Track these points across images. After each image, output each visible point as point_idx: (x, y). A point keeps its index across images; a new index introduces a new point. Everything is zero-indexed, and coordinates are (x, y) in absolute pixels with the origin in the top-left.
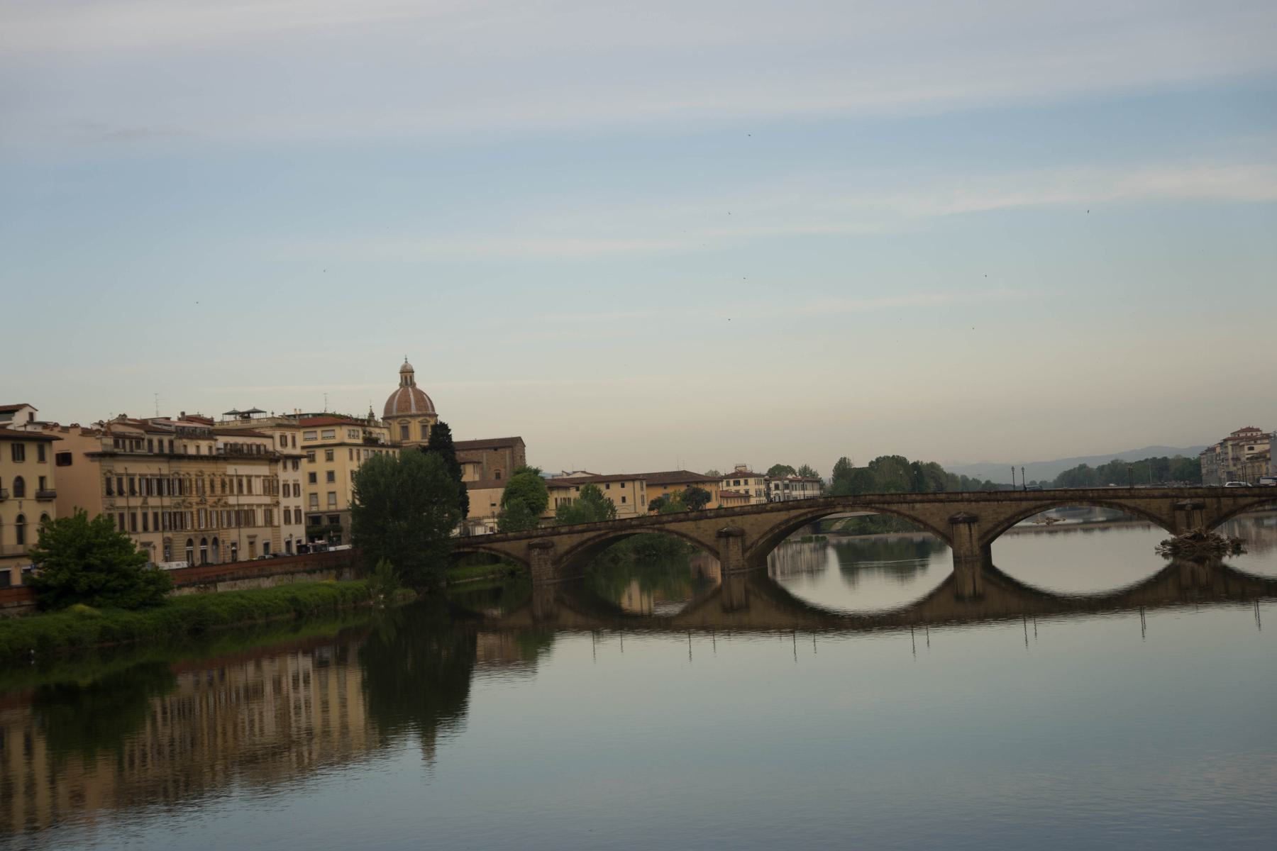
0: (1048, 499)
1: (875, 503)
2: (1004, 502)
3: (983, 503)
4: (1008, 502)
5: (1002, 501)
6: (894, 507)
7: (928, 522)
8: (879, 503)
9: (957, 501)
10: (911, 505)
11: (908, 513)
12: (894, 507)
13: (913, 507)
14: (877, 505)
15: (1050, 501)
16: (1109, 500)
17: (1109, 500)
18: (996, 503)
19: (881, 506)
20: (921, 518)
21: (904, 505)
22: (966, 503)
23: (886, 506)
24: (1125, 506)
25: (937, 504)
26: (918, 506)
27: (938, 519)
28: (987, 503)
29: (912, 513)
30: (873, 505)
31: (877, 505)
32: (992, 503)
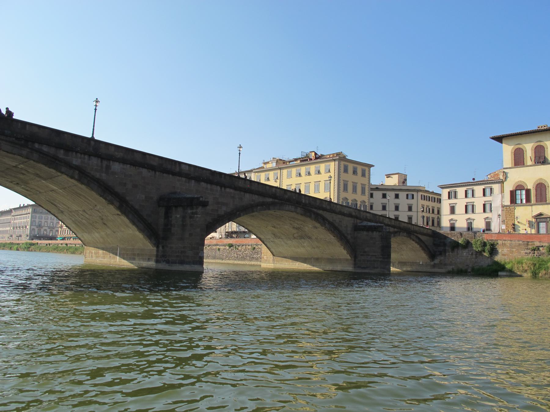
0: (270, 197)
1: (40, 143)
2: (228, 190)
3: (203, 184)
4: (232, 191)
5: (225, 187)
6: (76, 161)
7: (127, 198)
8: (49, 145)
9: (174, 174)
10: (105, 163)
11: (97, 175)
12: (76, 161)
13: (108, 167)
14: (45, 149)
15: (271, 200)
16: (315, 210)
17: (315, 210)
18: (219, 188)
19: (52, 151)
20: (119, 189)
21: (95, 161)
22: (184, 179)
23: (61, 154)
24: (327, 220)
25: (144, 171)
26: (116, 167)
27: (144, 196)
28: (209, 186)
29: (104, 176)
30: (37, 146)
31: (45, 149)
32: (214, 187)
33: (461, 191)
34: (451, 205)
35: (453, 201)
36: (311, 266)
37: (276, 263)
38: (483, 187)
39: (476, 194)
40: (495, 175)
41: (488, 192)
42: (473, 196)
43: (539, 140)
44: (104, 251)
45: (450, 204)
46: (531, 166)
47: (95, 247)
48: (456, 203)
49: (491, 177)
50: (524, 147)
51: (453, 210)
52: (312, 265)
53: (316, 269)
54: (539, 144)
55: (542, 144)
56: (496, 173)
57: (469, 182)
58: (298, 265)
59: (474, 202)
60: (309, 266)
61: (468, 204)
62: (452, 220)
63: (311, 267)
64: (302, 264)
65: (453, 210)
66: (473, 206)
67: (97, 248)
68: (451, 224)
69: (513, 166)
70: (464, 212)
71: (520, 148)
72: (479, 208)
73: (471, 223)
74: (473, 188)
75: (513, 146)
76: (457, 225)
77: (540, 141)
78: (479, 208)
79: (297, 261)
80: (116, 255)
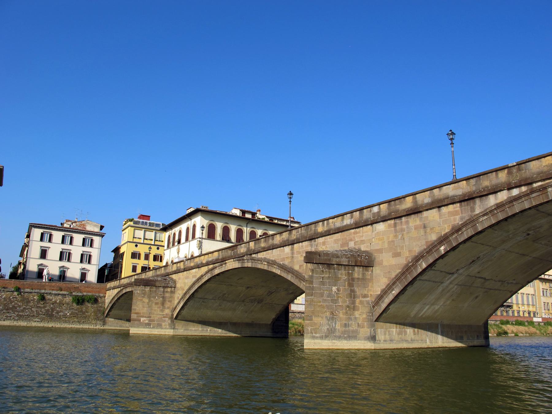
33: (57, 236)
34: (43, 248)
35: (45, 244)
36: (227, 332)
37: (177, 329)
38: (83, 236)
39: (75, 242)
40: (81, 224)
41: (88, 242)
42: (71, 243)
43: (227, 222)
44: (416, 330)
45: (41, 247)
46: (219, 241)
47: (396, 324)
48: (49, 248)
49: (77, 225)
50: (216, 223)
51: (44, 254)
52: (228, 331)
53: (239, 336)
54: (226, 225)
55: (228, 225)
56: (83, 223)
57: (56, 226)
58: (210, 331)
59: (71, 250)
60: (224, 331)
61: (84, 253)
62: (41, 265)
63: (227, 333)
64: (216, 329)
65: (44, 254)
66: (70, 253)
67: (400, 324)
68: (39, 269)
69: (207, 238)
70: (79, 261)
71: (213, 224)
72: (76, 257)
73: (64, 272)
74: (72, 235)
75: (208, 221)
76: (69, 274)
77: (227, 223)
78: (76, 257)
79: (209, 326)
80: (437, 333)
